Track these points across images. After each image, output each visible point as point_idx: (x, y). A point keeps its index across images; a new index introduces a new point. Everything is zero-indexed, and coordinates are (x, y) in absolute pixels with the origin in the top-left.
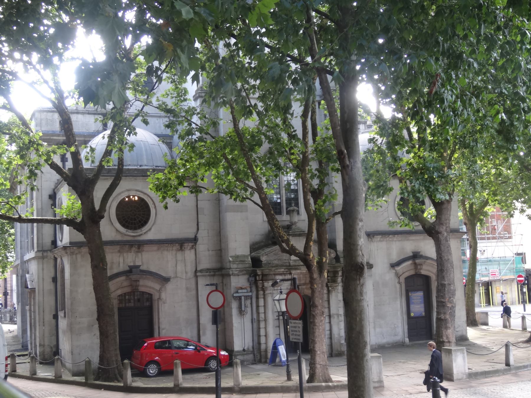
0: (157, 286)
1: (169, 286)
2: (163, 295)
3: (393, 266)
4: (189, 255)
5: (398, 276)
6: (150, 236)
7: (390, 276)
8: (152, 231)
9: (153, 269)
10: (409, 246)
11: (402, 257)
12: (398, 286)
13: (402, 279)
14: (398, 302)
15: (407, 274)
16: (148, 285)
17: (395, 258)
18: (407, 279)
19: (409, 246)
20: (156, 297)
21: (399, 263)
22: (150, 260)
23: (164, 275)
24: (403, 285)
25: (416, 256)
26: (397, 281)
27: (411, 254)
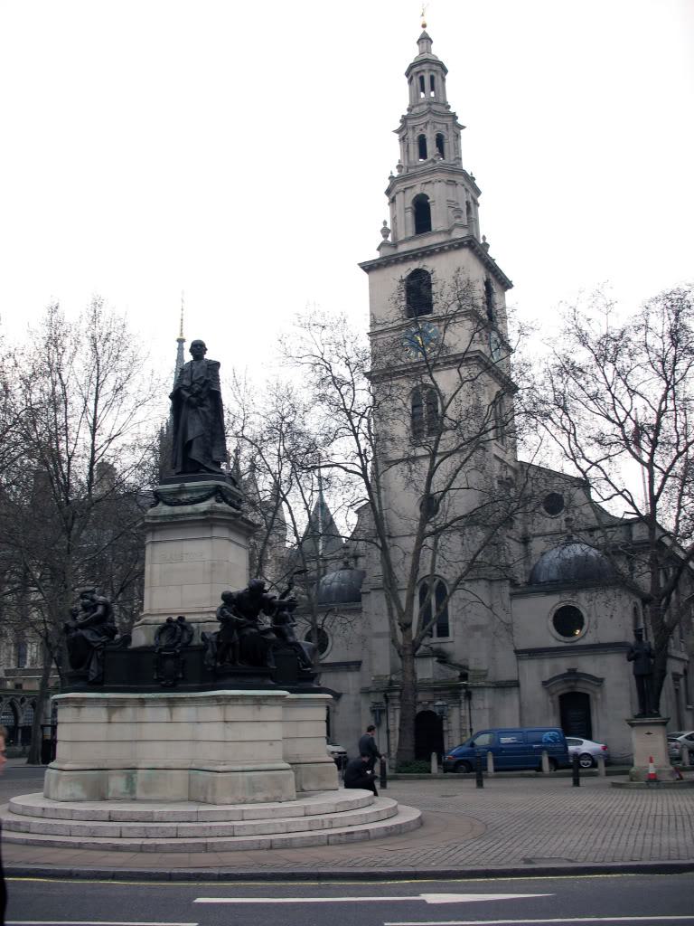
2: (337, 708)
3: (545, 683)
5: (552, 695)
6: (328, 660)
7: (540, 695)
10: (563, 665)
11: (556, 674)
12: (550, 704)
15: (561, 693)
18: (562, 698)
19: (563, 665)
21: (551, 680)
23: (338, 691)
24: (557, 704)
25: (573, 674)
26: (550, 699)
27: (566, 671)
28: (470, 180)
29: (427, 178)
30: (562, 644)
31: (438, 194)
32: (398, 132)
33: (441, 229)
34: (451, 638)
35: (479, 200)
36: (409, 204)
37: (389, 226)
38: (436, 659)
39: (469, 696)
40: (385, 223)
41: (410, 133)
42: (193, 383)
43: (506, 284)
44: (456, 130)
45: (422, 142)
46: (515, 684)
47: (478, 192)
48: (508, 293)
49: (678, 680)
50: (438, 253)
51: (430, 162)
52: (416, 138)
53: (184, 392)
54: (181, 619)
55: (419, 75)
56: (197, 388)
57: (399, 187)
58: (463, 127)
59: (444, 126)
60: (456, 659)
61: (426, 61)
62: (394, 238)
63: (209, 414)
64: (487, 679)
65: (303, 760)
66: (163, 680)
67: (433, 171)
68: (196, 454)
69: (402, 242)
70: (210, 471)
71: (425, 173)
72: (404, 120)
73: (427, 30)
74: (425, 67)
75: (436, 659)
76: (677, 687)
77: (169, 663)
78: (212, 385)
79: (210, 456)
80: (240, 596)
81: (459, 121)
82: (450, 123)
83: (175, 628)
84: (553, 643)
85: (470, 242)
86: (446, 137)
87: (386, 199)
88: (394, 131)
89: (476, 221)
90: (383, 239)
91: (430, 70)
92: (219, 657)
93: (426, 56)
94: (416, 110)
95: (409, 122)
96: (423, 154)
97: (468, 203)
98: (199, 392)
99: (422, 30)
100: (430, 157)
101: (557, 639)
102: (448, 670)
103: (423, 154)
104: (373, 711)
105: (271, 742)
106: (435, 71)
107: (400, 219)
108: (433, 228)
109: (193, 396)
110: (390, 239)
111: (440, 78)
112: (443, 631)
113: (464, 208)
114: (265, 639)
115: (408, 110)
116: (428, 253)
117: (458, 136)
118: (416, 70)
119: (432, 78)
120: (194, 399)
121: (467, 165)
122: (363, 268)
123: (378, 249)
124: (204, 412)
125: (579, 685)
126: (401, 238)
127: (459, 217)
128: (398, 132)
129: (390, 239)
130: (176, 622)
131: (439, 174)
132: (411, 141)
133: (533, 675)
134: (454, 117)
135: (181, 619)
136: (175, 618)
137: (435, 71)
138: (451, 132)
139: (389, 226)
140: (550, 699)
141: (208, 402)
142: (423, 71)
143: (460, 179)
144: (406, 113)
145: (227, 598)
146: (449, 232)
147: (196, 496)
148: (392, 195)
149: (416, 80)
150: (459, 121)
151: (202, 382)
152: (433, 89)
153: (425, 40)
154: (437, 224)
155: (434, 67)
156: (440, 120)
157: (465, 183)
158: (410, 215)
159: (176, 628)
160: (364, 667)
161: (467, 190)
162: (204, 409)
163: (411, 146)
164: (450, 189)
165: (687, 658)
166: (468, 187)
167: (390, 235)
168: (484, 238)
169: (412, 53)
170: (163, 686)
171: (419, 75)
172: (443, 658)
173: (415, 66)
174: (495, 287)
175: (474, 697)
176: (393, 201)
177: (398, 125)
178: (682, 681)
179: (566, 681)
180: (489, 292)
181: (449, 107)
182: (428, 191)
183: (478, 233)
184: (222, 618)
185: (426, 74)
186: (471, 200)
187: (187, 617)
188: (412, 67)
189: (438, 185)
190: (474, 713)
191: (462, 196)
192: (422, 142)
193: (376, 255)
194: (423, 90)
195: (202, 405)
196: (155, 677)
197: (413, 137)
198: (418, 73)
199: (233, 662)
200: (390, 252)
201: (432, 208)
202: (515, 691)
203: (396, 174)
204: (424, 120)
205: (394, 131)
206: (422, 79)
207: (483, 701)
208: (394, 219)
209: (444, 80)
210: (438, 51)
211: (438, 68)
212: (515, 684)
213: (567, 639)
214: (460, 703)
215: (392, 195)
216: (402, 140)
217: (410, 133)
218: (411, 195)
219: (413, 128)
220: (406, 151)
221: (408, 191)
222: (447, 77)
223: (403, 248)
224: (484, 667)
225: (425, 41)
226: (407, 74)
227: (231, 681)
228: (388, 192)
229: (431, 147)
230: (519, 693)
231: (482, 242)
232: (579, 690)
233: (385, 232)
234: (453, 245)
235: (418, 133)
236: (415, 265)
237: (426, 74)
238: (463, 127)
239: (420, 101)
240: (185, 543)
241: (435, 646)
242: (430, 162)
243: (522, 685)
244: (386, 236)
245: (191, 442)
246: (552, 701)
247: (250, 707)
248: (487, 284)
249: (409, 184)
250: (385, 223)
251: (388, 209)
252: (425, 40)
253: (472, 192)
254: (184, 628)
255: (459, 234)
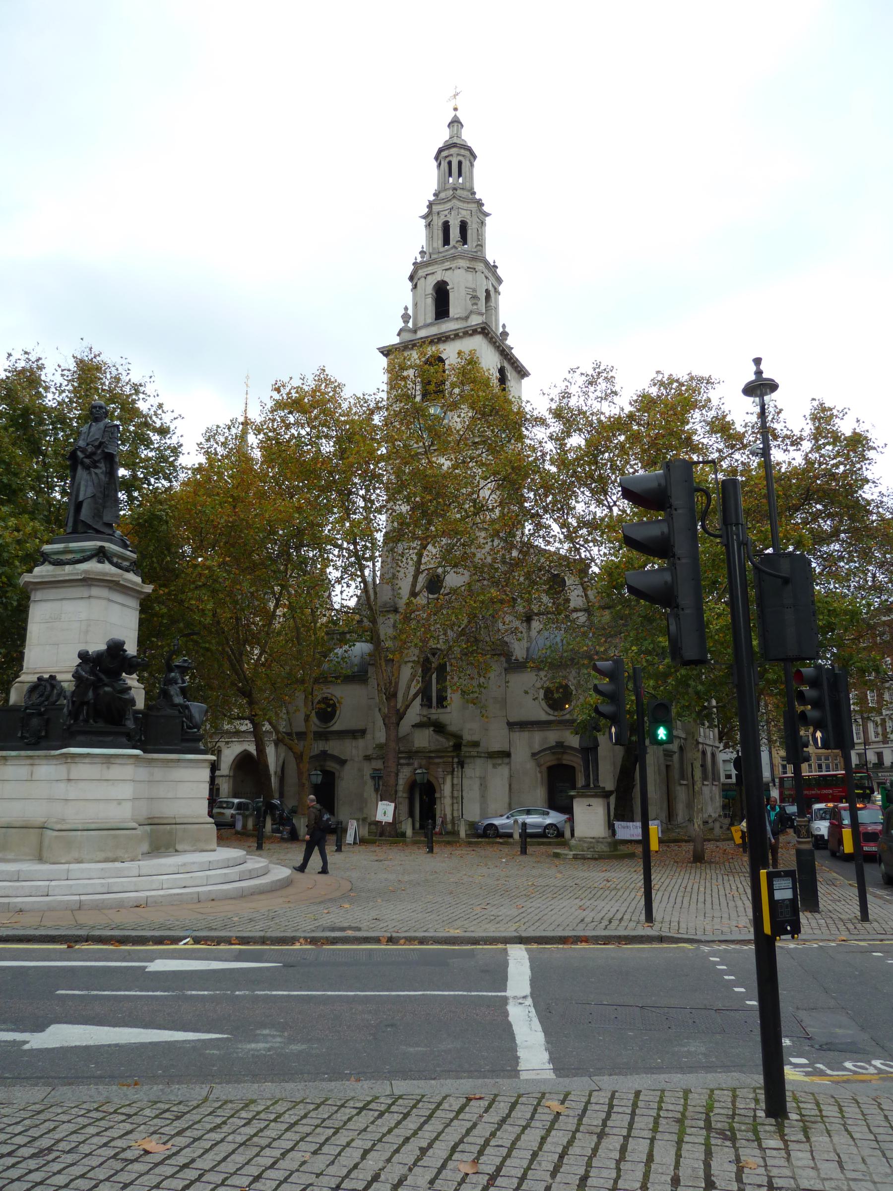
0: (337, 766)
1: (347, 767)
3: (534, 755)
4: (361, 743)
6: (336, 728)
7: (530, 765)
8: (337, 725)
9: (336, 753)
10: (552, 737)
12: (539, 775)
13: (544, 769)
14: (539, 791)
15: (549, 764)
16: (331, 766)
17: (537, 748)
18: (550, 769)
19: (552, 737)
20: (337, 774)
22: (334, 747)
24: (545, 775)
25: (560, 745)
27: (554, 744)
28: (493, 269)
29: (447, 265)
30: (552, 718)
31: (460, 283)
32: (424, 217)
33: (458, 316)
34: (449, 709)
35: (501, 288)
36: (430, 289)
37: (410, 312)
38: (432, 729)
39: (462, 764)
40: (406, 309)
41: (435, 218)
42: (88, 445)
43: (522, 373)
44: (481, 216)
45: (446, 227)
46: (507, 755)
47: (499, 280)
48: (525, 381)
49: (671, 756)
50: (453, 339)
51: (452, 248)
52: (440, 224)
53: (79, 453)
54: (52, 678)
55: (448, 159)
56: (90, 449)
57: (421, 273)
58: (487, 215)
59: (469, 212)
60: (452, 728)
61: (454, 145)
62: (414, 324)
63: (102, 477)
64: (480, 749)
65: (178, 821)
66: (27, 738)
67: (454, 258)
68: (85, 514)
69: (420, 328)
70: (98, 532)
71: (443, 262)
72: (430, 205)
73: (458, 114)
74: (453, 151)
75: (432, 729)
76: (669, 763)
77: (35, 721)
78: (107, 448)
79: (101, 517)
80: (99, 656)
81: (485, 208)
82: (474, 210)
83: (46, 686)
84: (544, 717)
85: (483, 329)
86: (469, 223)
87: (410, 285)
88: (421, 217)
89: (496, 309)
90: (403, 325)
91: (458, 155)
92: (74, 714)
93: (455, 140)
94: (442, 195)
95: (434, 207)
96: (446, 241)
97: (487, 291)
98: (94, 454)
99: (453, 113)
100: (452, 243)
101: (546, 712)
102: (442, 739)
103: (446, 241)
104: (373, 778)
105: (119, 802)
106: (463, 156)
107: (421, 305)
108: (451, 313)
109: (86, 457)
110: (410, 325)
111: (468, 162)
112: (442, 701)
113: (483, 296)
114: (120, 699)
115: (435, 195)
116: (443, 338)
117: (483, 223)
118: (444, 154)
119: (460, 163)
120: (87, 461)
121: (491, 256)
122: (382, 352)
123: (399, 335)
124: (96, 474)
125: (565, 757)
126: (420, 324)
127: (476, 304)
128: (424, 217)
129: (410, 325)
130: (46, 680)
131: (460, 261)
132: (435, 227)
133: (523, 747)
134: (480, 203)
135: (52, 678)
136: (46, 676)
137: (463, 156)
138: (475, 219)
139: (410, 312)
140: (538, 769)
141: (102, 465)
142: (451, 155)
143: (480, 266)
144: (432, 198)
145: (83, 656)
146: (466, 318)
147: (78, 556)
148: (415, 281)
149: (444, 164)
150: (485, 208)
151: (97, 443)
152: (460, 175)
153: (456, 123)
154: (455, 309)
155: (463, 152)
156: (465, 206)
157: (486, 272)
158: (430, 302)
159: (45, 687)
160: (368, 736)
161: (487, 278)
162: (97, 471)
163: (435, 232)
164: (470, 276)
165: (683, 736)
166: (489, 275)
167: (411, 321)
168: (504, 326)
169: (443, 136)
170: (27, 744)
171: (448, 159)
172: (439, 728)
173: (443, 150)
174: (510, 374)
175: (466, 766)
176: (415, 287)
177: (425, 210)
178: (676, 757)
179: (553, 753)
180: (503, 380)
181: (474, 193)
182: (447, 277)
183: (497, 321)
184: (76, 675)
185: (455, 158)
186: (491, 288)
187: (59, 677)
188: (440, 151)
189: (457, 271)
190: (466, 782)
191: (483, 284)
192: (446, 227)
193: (396, 340)
194: (450, 175)
195: (96, 467)
196: (19, 735)
197: (438, 222)
198: (446, 157)
199: (86, 721)
200: (408, 337)
201: (451, 295)
202: (506, 760)
203: (419, 260)
204: (448, 206)
205: (421, 217)
206: (450, 163)
207: (474, 770)
208: (415, 305)
209: (472, 165)
210: (468, 136)
211: (467, 153)
212: (507, 755)
213: (556, 714)
214: (453, 771)
215: (415, 281)
216: (429, 225)
217: (435, 218)
218: (432, 281)
219: (438, 213)
220: (430, 238)
221: (429, 277)
222: (476, 163)
223: (422, 334)
224: (475, 738)
225: (456, 124)
226: (436, 158)
227: (80, 738)
228: (411, 278)
229: (455, 233)
230: (509, 763)
231: (501, 330)
232: (564, 762)
233: (406, 317)
234: (467, 332)
235: (443, 219)
236: (430, 350)
237: (455, 158)
238: (487, 215)
239: (447, 186)
240: (64, 602)
241: (434, 717)
242: (452, 248)
243: (513, 755)
244: (406, 322)
245: (81, 502)
246: (541, 772)
247: (88, 766)
248: (502, 371)
249: (430, 269)
250: (406, 309)
251: (410, 295)
252: (456, 123)
253: (492, 280)
254: (53, 687)
255: (475, 320)
